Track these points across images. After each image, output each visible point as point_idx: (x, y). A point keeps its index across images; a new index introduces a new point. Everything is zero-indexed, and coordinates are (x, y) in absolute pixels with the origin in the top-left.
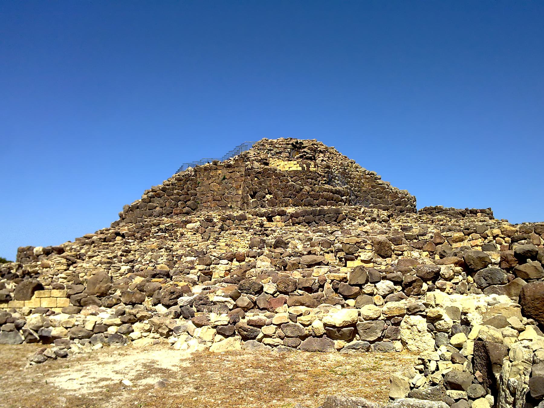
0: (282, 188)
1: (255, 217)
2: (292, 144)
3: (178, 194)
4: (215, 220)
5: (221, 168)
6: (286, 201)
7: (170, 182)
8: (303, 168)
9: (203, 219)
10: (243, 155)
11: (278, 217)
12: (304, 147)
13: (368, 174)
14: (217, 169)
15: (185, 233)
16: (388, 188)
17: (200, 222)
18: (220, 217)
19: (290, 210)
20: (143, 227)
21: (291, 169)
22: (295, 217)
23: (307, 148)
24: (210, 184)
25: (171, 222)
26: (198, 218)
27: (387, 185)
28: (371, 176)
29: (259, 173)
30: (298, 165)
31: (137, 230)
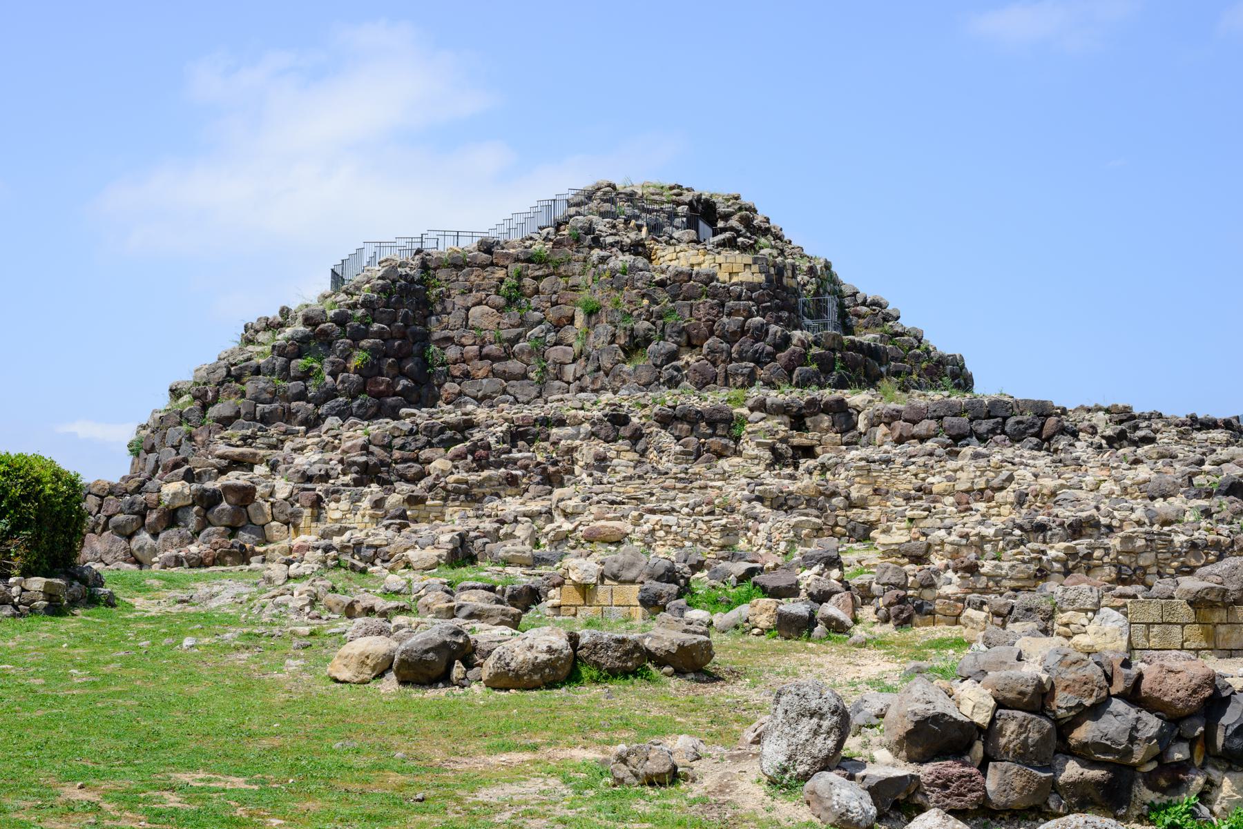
0: (734, 333)
1: (758, 415)
2: (690, 204)
3: (379, 334)
4: (635, 420)
5: (507, 262)
6: (745, 371)
7: (355, 298)
8: (769, 280)
9: (600, 414)
10: (581, 228)
11: (826, 420)
12: (726, 217)
13: (864, 303)
14: (492, 264)
15: (610, 454)
16: (918, 347)
17: (593, 424)
18: (647, 411)
19: (856, 398)
20: (417, 433)
21: (735, 280)
22: (905, 421)
23: (736, 217)
24: (468, 309)
25: (506, 420)
26: (581, 413)
27: (916, 337)
28: (874, 310)
29: (662, 284)
30: (755, 268)
31: (398, 442)
